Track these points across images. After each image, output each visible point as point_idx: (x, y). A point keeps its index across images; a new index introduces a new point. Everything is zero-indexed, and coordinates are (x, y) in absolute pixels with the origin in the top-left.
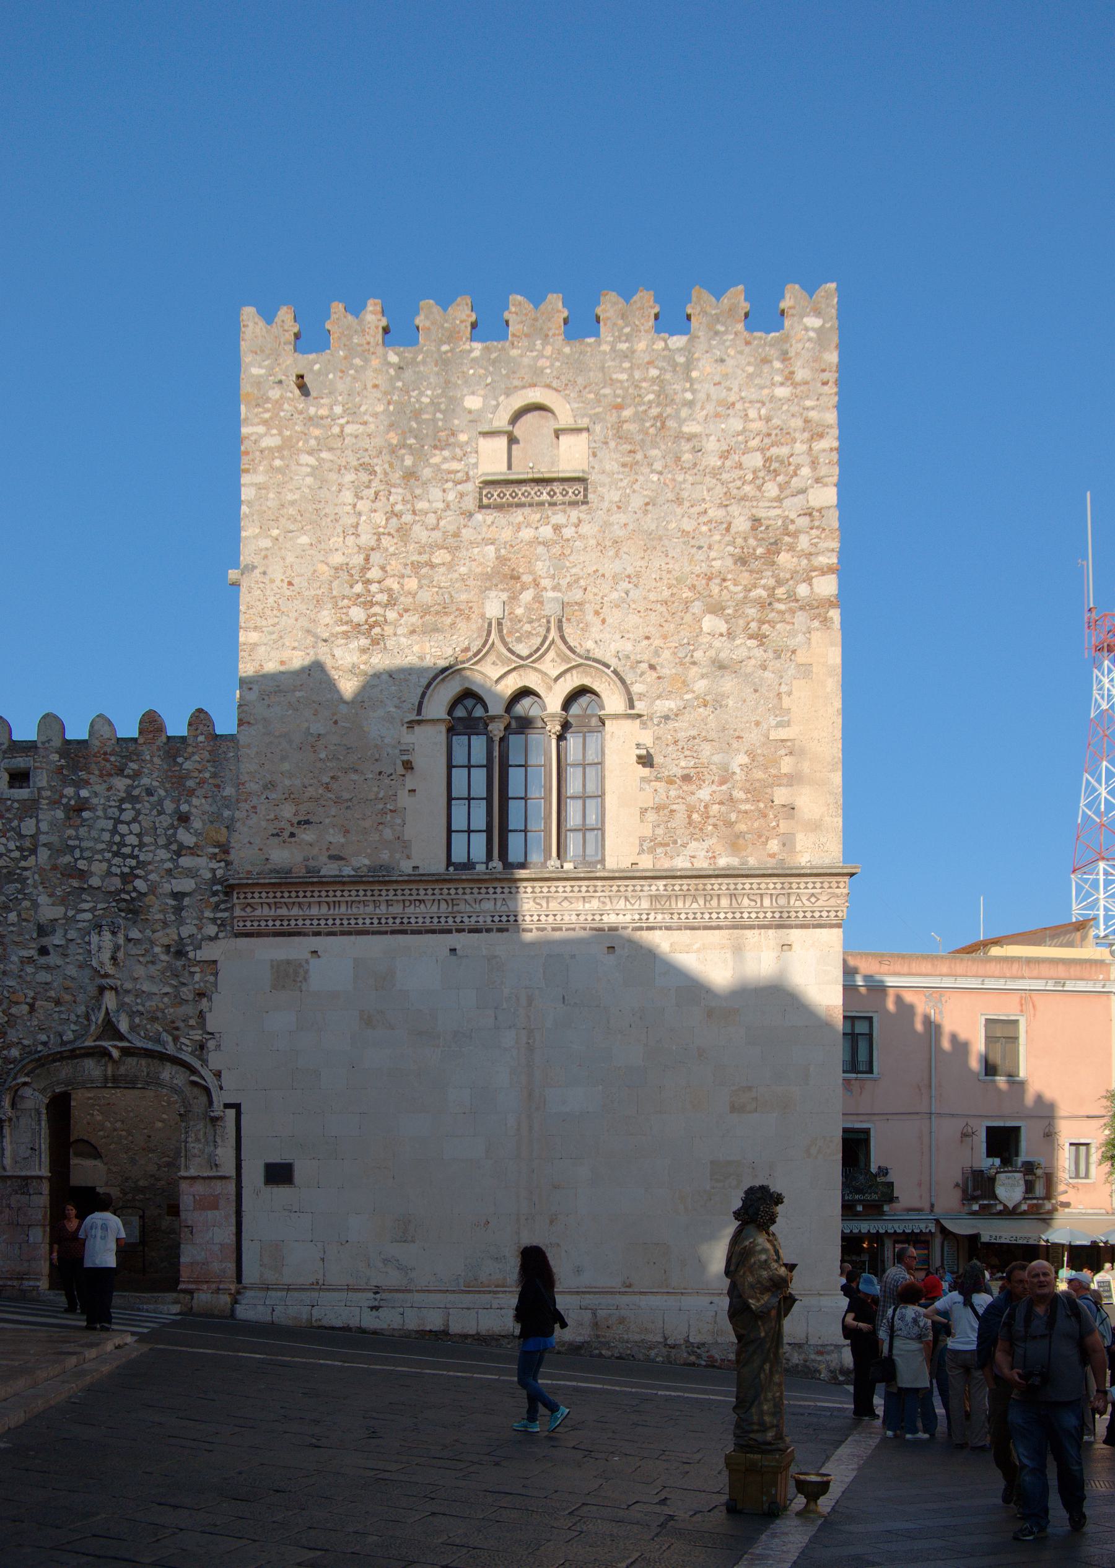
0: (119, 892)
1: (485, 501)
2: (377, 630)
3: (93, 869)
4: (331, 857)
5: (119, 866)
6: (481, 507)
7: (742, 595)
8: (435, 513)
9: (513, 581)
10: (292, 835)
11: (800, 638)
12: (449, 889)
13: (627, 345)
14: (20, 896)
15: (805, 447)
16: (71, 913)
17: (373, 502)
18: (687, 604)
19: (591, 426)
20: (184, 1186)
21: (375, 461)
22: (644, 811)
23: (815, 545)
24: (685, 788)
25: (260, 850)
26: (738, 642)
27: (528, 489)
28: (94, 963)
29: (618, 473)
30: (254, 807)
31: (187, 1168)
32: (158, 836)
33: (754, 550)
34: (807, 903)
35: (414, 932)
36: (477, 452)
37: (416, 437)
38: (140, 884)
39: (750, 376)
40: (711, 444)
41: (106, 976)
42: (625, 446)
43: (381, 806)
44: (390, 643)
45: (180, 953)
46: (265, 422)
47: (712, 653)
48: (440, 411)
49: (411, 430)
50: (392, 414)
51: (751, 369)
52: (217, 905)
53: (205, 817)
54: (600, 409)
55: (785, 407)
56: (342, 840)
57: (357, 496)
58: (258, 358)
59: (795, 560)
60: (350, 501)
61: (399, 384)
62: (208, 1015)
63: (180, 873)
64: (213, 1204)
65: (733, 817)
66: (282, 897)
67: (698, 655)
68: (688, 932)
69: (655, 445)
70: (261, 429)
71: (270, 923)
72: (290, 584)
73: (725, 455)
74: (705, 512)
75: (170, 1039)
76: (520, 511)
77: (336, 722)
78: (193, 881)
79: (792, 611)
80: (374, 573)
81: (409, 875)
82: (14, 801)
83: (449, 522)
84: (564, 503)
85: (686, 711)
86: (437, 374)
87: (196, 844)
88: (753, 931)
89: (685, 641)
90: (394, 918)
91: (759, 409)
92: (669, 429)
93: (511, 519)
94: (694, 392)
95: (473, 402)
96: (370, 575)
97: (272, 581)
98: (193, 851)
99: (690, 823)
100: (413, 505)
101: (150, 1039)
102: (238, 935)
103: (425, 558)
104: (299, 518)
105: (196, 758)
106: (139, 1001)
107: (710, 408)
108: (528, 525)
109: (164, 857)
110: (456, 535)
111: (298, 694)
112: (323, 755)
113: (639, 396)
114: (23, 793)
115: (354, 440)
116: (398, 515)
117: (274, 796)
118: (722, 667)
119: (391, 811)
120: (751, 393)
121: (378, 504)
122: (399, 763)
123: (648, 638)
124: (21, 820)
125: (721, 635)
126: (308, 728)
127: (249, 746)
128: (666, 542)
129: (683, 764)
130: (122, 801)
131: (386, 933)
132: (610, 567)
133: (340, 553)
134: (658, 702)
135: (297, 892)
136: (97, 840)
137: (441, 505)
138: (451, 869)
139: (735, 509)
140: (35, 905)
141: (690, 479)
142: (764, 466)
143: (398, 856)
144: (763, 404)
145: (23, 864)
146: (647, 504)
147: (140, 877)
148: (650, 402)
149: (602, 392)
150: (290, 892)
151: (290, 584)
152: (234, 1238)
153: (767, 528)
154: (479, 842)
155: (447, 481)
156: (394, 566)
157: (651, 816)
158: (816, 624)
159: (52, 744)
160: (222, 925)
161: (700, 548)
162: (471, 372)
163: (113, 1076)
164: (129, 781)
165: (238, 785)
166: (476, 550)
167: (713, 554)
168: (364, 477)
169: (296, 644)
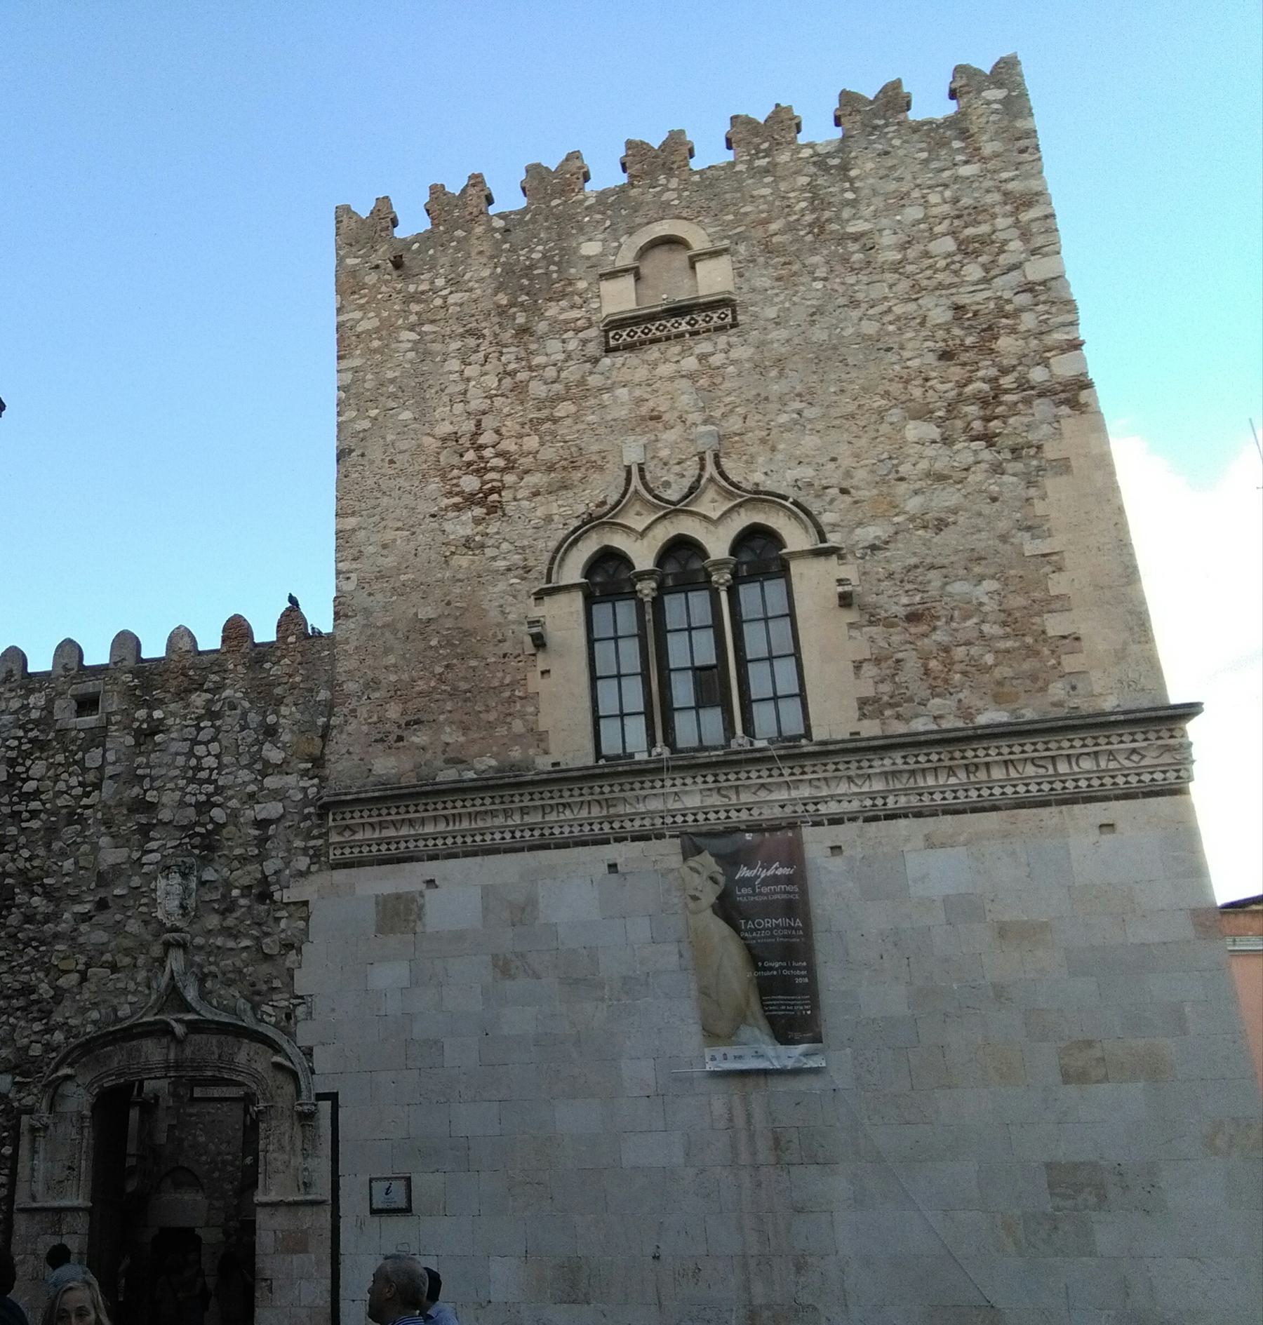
0: (197, 823)
1: (612, 343)
2: (495, 497)
3: (164, 800)
5: (195, 795)
6: (609, 350)
7: (953, 393)
8: (555, 365)
9: (651, 423)
10: (400, 739)
11: (1045, 429)
12: (601, 787)
13: (767, 160)
14: (79, 840)
15: (1010, 221)
16: (136, 855)
17: (482, 365)
18: (881, 414)
19: (733, 247)
20: (262, 1217)
21: (484, 325)
22: (858, 666)
23: (1045, 321)
24: (913, 630)
25: (361, 759)
26: (958, 446)
27: (663, 322)
28: (160, 914)
29: (773, 288)
30: (354, 711)
31: (267, 1191)
32: (240, 755)
34: (1127, 763)
35: (558, 846)
37: (527, 294)
38: (216, 813)
39: (926, 162)
40: (887, 239)
41: (176, 929)
42: (777, 260)
43: (507, 694)
44: (510, 508)
45: (265, 896)
47: (924, 465)
48: (554, 264)
49: (522, 288)
50: (501, 275)
52: (310, 830)
53: (295, 728)
54: (742, 229)
56: (462, 739)
57: (464, 362)
58: (354, 249)
59: (1021, 342)
61: (507, 246)
62: (296, 972)
63: (267, 795)
64: (296, 1244)
65: (989, 659)
66: (389, 814)
67: (904, 469)
68: (949, 817)
69: (814, 251)
70: (358, 315)
71: (374, 848)
73: (903, 247)
75: (248, 1006)
76: (655, 347)
77: (449, 603)
79: (1028, 401)
80: (487, 438)
81: (549, 772)
82: (79, 731)
83: (573, 372)
84: (708, 330)
85: (899, 537)
86: (548, 228)
87: (285, 761)
88: (1049, 809)
89: (885, 456)
90: (532, 830)
91: (942, 193)
92: (832, 232)
93: (646, 357)
94: (854, 190)
98: (280, 769)
99: (927, 672)
101: (225, 1009)
102: (336, 866)
103: (545, 413)
104: (400, 394)
105: (286, 661)
106: (212, 959)
107: (878, 202)
108: (666, 361)
109: (246, 779)
110: (582, 382)
111: (403, 577)
113: (788, 206)
114: (90, 720)
115: (458, 309)
116: (512, 374)
117: (377, 695)
118: (941, 478)
120: (927, 178)
121: (488, 367)
122: (528, 640)
123: (833, 459)
124: (86, 751)
125: (934, 442)
126: (416, 614)
127: (347, 642)
129: (905, 600)
130: (200, 718)
131: (522, 850)
133: (447, 423)
134: (858, 531)
135: (407, 806)
136: (171, 765)
137: (561, 357)
138: (602, 762)
140: (96, 848)
141: (865, 279)
143: (531, 752)
144: (946, 186)
145: (85, 801)
146: (813, 314)
147: (219, 806)
148: (803, 210)
149: (742, 210)
150: (398, 807)
151: (392, 462)
152: (327, 1297)
153: (976, 314)
154: (636, 728)
156: (511, 426)
157: (869, 670)
158: (1064, 410)
159: (125, 663)
160: (316, 855)
161: (889, 350)
163: (176, 1061)
164: (209, 696)
165: (332, 685)
166: (606, 396)
167: (906, 354)
168: (472, 342)
169: (400, 524)
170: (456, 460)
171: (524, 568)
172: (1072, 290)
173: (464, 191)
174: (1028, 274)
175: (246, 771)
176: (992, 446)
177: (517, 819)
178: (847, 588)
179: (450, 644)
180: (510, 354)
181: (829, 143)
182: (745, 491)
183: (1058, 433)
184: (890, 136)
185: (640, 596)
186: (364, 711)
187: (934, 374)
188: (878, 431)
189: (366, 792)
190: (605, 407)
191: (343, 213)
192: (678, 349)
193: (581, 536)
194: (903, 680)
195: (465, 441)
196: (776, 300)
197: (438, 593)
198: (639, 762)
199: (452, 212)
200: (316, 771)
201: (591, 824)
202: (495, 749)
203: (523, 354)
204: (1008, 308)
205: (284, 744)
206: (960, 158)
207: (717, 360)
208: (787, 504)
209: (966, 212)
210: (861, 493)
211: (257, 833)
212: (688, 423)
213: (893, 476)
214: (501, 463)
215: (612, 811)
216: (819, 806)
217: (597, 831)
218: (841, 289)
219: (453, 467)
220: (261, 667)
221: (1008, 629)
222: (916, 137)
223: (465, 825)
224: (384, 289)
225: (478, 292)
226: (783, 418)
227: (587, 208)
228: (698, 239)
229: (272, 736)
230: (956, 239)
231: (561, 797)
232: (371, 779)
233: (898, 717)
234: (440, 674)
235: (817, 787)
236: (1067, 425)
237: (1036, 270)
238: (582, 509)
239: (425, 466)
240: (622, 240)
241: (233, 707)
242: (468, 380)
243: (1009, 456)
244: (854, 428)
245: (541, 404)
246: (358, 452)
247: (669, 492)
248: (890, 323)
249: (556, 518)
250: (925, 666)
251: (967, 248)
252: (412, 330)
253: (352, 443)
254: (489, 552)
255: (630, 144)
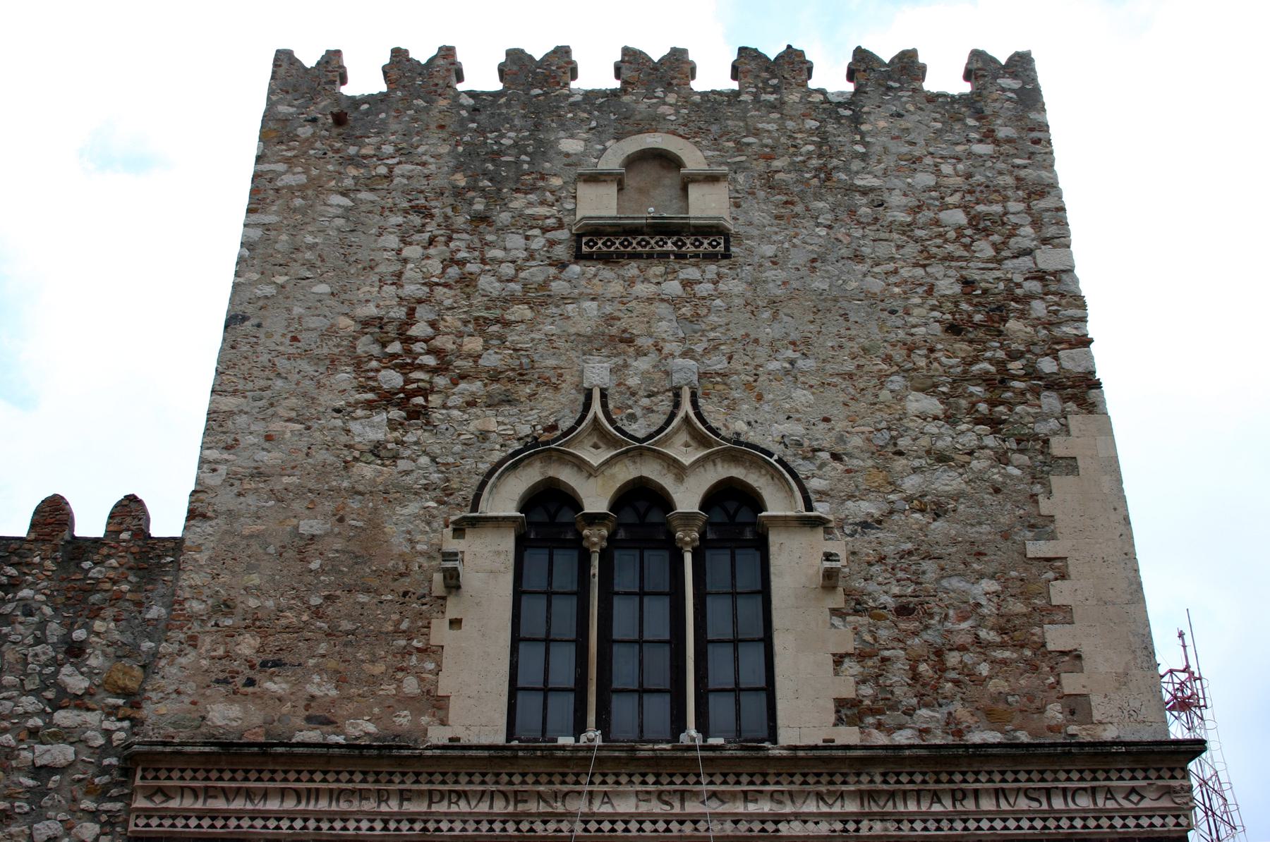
1: (585, 249)
2: (419, 400)
4: (309, 719)
6: (579, 257)
7: (959, 370)
8: (513, 262)
9: (623, 346)
10: (251, 682)
18: (882, 379)
22: (839, 660)
23: (1056, 312)
24: (902, 626)
25: (194, 703)
26: (964, 427)
27: (647, 238)
29: (771, 225)
32: (27, 675)
33: (970, 316)
36: (575, 197)
37: (491, 180)
39: (937, 132)
40: (896, 199)
42: (778, 197)
43: (403, 642)
44: (436, 416)
46: (287, 160)
47: (925, 442)
48: (526, 154)
49: (485, 173)
51: (939, 125)
54: (743, 158)
55: (989, 164)
56: (334, 693)
57: (403, 241)
58: (289, 97)
59: (1029, 329)
60: (395, 246)
67: (903, 443)
70: (281, 167)
72: (294, 339)
74: (896, 272)
76: (634, 264)
77: (341, 520)
78: (72, 749)
84: (696, 256)
86: (524, 116)
87: (88, 692)
89: (884, 425)
92: (839, 181)
95: (571, 145)
96: (414, 331)
97: (269, 335)
98: (80, 702)
100: (482, 252)
104: (319, 263)
105: (113, 562)
109: (30, 709)
112: (315, 565)
113: (795, 146)
115: (405, 181)
116: (462, 263)
117: (229, 622)
118: (942, 458)
119: (419, 650)
121: (432, 251)
122: (438, 577)
123: (826, 420)
125: (936, 418)
126: (297, 527)
127: (198, 548)
128: (844, 304)
129: (896, 590)
132: (768, 332)
133: (372, 305)
134: (850, 504)
138: (515, 743)
139: (937, 270)
142: (970, 223)
143: (425, 719)
144: (959, 160)
146: (814, 260)
148: (809, 153)
149: (745, 140)
155: (532, 228)
158: (1071, 406)
161: (893, 312)
162: (570, 115)
165: (174, 603)
166: (570, 307)
168: (417, 220)
169: (293, 414)
170: (376, 350)
171: (444, 490)
172: (1081, 286)
173: (431, 60)
174: (1038, 261)
175: (32, 699)
176: (999, 432)
177: (394, 806)
178: (834, 564)
179: (335, 570)
180: (460, 244)
181: (841, 94)
182: (723, 438)
183: (1065, 429)
184: (904, 99)
185: (585, 544)
186: (208, 639)
187: (939, 346)
188: (877, 396)
189: (194, 744)
190: (569, 318)
191: (284, 60)
192: (659, 269)
193: (521, 460)
194: (888, 682)
195: (391, 329)
196: (775, 238)
197: (328, 506)
198: (563, 748)
199: (414, 79)
200: (129, 712)
201: (491, 822)
202: (376, 710)
203: (479, 245)
204: (1018, 291)
205: (91, 668)
206: (973, 135)
207: (705, 289)
208: (772, 460)
209: (979, 189)
210: (855, 462)
211: (31, 783)
212: (665, 351)
213: (891, 449)
214: (431, 361)
215: (521, 807)
216: (780, 826)
217: (497, 832)
218: (846, 240)
219: (371, 357)
220: (78, 566)
221: (1006, 638)
222: (931, 106)
223: (323, 805)
224: (318, 145)
225: (433, 167)
226: (774, 365)
227: (571, 105)
228: (694, 158)
229: (77, 656)
230: (968, 213)
231: (456, 782)
232: (204, 730)
233: (879, 726)
234: (318, 607)
235: (780, 802)
236: (1075, 422)
237: (1047, 259)
238: (525, 430)
239: (336, 351)
240: (608, 144)
241: (29, 612)
242: (405, 261)
243: (1014, 446)
244: (851, 390)
245: (492, 302)
246: (254, 321)
247: (634, 426)
248: (896, 285)
249: (493, 436)
250: (913, 669)
251: (978, 224)
252: (344, 194)
253: (249, 310)
254: (403, 465)
255: (626, 51)
